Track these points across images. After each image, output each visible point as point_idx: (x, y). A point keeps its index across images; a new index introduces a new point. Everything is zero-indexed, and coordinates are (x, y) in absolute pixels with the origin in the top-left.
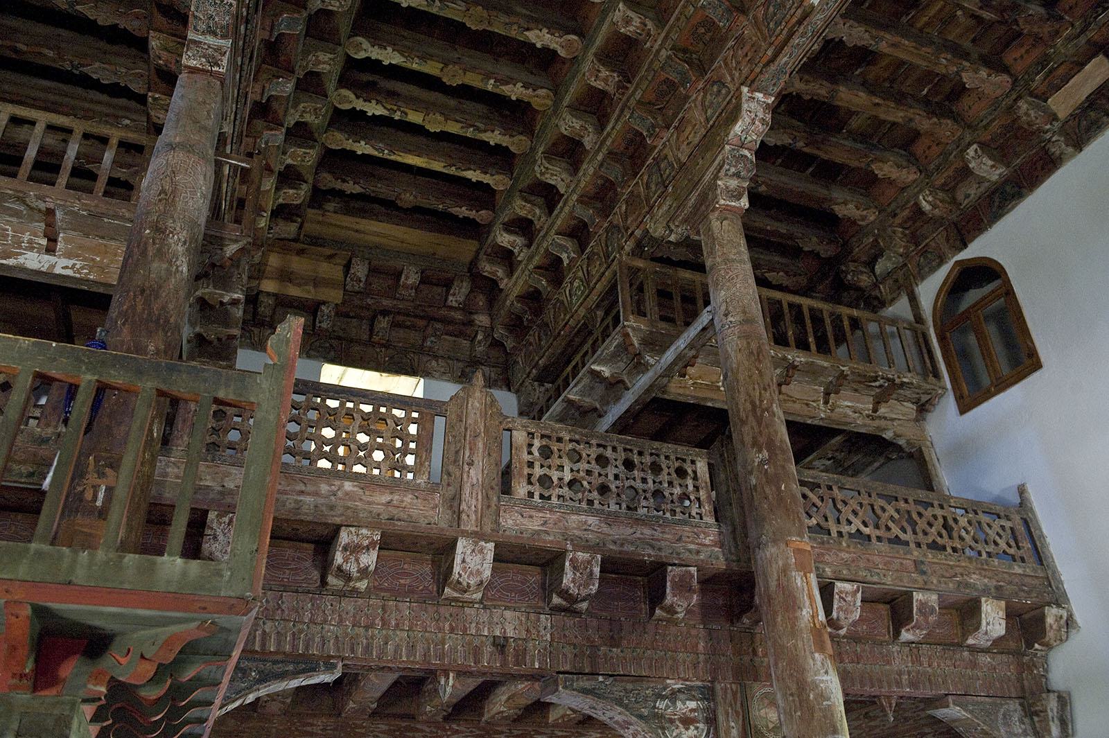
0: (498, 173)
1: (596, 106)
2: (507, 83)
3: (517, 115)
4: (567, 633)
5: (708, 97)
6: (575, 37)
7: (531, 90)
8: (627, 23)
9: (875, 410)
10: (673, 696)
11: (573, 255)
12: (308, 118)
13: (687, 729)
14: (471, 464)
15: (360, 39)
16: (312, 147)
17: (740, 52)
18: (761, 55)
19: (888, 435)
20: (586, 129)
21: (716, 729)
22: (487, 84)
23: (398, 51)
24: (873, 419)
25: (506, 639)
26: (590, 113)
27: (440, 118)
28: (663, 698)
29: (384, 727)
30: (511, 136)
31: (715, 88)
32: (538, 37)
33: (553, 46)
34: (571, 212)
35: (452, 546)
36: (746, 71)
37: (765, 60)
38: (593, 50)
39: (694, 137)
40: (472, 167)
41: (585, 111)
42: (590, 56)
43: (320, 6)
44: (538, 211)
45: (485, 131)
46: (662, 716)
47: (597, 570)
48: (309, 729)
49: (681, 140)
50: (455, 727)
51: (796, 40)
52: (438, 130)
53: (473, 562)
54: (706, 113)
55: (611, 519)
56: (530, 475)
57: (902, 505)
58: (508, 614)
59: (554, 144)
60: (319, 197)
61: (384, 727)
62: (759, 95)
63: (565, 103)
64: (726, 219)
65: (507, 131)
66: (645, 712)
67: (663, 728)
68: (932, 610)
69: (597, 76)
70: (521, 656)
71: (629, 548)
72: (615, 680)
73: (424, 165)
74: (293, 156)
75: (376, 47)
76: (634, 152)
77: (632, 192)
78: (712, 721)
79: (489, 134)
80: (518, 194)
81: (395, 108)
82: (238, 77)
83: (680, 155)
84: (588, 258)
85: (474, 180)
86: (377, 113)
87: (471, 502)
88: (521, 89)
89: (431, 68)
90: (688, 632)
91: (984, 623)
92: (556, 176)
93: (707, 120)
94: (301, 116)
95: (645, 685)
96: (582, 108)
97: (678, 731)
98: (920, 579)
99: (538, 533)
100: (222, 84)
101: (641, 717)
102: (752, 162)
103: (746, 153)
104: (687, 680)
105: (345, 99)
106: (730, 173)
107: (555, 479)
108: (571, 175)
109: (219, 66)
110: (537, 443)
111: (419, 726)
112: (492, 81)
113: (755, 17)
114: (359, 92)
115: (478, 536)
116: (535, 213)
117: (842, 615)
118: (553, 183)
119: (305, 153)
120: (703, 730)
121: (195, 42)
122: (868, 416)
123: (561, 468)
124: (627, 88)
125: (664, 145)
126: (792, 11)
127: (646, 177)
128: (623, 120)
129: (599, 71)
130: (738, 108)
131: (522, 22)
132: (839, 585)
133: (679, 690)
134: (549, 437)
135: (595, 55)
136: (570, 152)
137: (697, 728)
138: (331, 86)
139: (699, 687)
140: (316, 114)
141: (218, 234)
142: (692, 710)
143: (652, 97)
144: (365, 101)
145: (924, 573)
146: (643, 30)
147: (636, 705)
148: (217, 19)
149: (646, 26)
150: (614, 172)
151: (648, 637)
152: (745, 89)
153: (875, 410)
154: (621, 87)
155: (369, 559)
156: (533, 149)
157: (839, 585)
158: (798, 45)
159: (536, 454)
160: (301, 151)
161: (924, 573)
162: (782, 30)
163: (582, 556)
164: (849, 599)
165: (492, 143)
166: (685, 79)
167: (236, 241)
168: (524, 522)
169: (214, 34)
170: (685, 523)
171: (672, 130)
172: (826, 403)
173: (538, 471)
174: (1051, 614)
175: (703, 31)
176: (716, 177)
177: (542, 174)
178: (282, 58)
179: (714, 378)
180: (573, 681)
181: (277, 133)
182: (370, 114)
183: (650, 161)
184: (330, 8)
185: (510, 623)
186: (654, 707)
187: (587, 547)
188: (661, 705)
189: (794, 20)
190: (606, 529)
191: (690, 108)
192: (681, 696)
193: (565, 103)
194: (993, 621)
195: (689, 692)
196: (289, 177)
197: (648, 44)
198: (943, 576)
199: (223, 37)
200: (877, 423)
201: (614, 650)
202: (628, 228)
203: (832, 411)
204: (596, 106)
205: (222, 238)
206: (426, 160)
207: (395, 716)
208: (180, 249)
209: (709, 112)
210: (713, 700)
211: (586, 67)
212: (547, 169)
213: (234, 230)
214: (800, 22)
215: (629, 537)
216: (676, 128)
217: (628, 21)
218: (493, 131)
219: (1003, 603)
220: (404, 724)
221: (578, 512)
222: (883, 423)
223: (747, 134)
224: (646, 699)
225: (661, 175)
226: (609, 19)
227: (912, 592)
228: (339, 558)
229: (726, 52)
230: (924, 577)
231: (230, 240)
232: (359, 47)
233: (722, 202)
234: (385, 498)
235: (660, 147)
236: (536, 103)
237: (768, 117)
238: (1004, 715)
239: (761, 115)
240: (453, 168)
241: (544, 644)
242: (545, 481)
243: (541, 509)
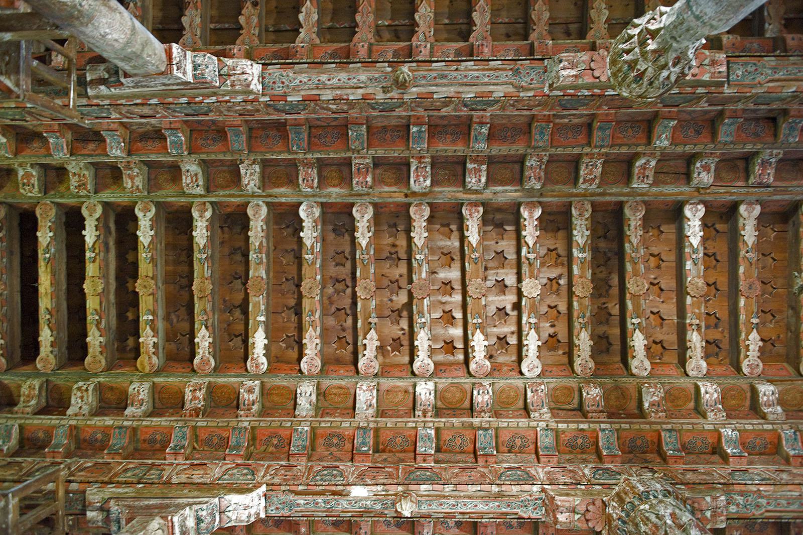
0: (55, 356)
1: (167, 402)
2: (153, 329)
3: (125, 347)
5: (235, 471)
6: (213, 365)
7: (154, 350)
8: (249, 391)
11: (5, 448)
12: (74, 181)
15: (153, 210)
16: (40, 192)
17: (283, 472)
18: (296, 483)
20: (141, 405)
22: (147, 315)
23: (152, 239)
26: (154, 402)
27: (100, 289)
30: (101, 353)
31: (245, 471)
32: (204, 336)
33: (201, 351)
34: (54, 427)
36: (277, 480)
37: (294, 488)
38: (212, 380)
39: (199, 478)
40: (55, 333)
41: (154, 399)
42: (207, 380)
43: (183, 170)
44: (33, 402)
45: (99, 329)
49: (186, 472)
51: (320, 499)
52: (86, 291)
54: (222, 476)
59: (112, 389)
63: (156, 380)
64: (163, 531)
65: (104, 347)
69: (195, 390)
73: (42, 290)
74: (28, 175)
75: (150, 223)
76: (149, 447)
77: (109, 464)
79: (97, 333)
80: (44, 379)
81: (97, 251)
82: (139, 101)
83: (174, 477)
84: (10, 463)
86: (87, 239)
88: (152, 343)
89: (145, 268)
92: (81, 401)
93: (219, 479)
94: (75, 174)
96: (156, 396)
100: (162, 73)
102: (213, 528)
105: (92, 212)
106: (200, 513)
108: (89, 412)
109: (177, 70)
112: (151, 317)
113: (311, 467)
114: (102, 220)
116: (29, 401)
118: (73, 401)
119: (33, 185)
121: (185, 56)
124: (198, 416)
125: (172, 464)
126: (338, 483)
127: (131, 466)
128: (174, 424)
129: (200, 390)
130: (250, 490)
131: (210, 321)
135: (210, 383)
136: (113, 402)
138: (107, 196)
140: (79, 186)
141: (21, 70)
143: (203, 436)
144: (96, 226)
146: (248, 405)
148: (207, 70)
149: (253, 405)
150: (118, 441)
152: (264, 488)
154: (197, 412)
156: (96, 375)
158: (317, 504)
160: (35, 181)
162: (322, 485)
165: (88, 339)
166: (237, 447)
167: (17, 85)
169: (195, 68)
171: (188, 462)
175: (275, 443)
176: (190, 505)
177: (79, 389)
178: (139, 144)
181: (66, 151)
182: (84, 233)
183: (150, 462)
184: (184, 177)
189: (334, 488)
191: (216, 464)
193: (156, 380)
197: (242, 413)
199: (194, 76)
202: (73, 476)
204: (167, 402)
206: (49, 291)
209: (226, 477)
211: (195, 380)
212: (87, 390)
213: (26, 83)
214: (334, 493)
216: (192, 465)
217: (250, 391)
218: (101, 336)
223: (235, 509)
225: (145, 474)
226: (242, 379)
229: (276, 464)
231: (18, 80)
232: (146, 210)
233: (175, 519)
235: (167, 462)
236: (143, 360)
237: (253, 519)
239: (253, 511)
240: (48, 317)
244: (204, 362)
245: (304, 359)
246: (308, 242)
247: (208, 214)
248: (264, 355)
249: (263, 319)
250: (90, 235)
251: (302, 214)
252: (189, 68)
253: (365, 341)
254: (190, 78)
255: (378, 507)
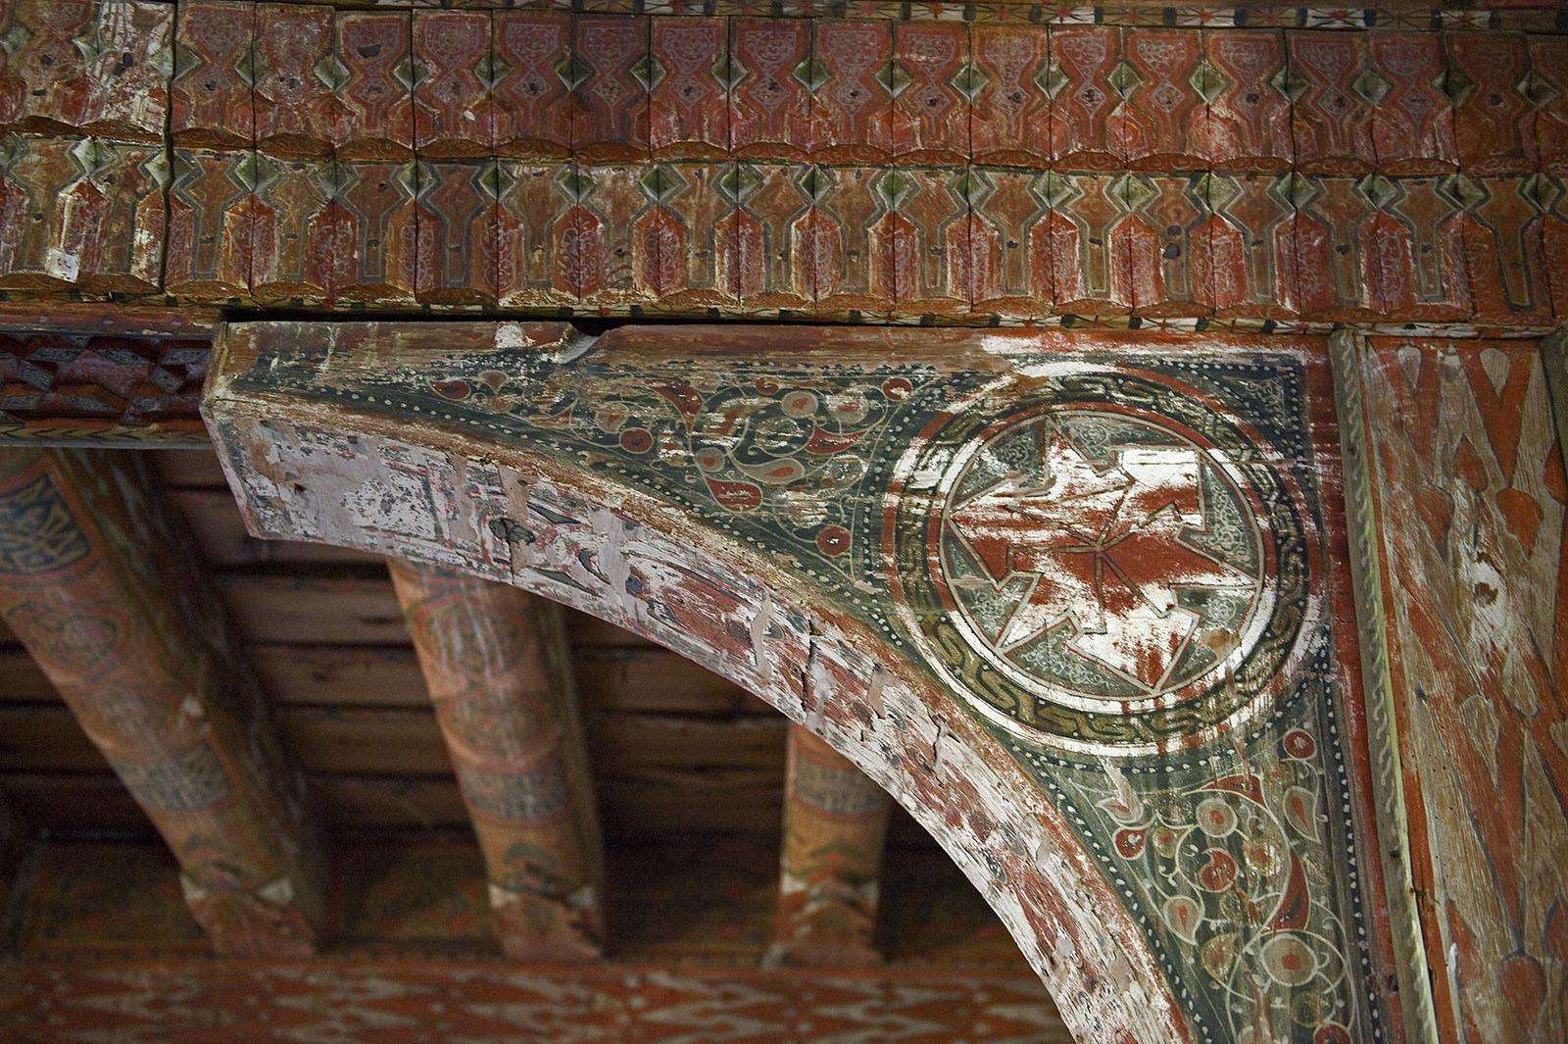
4: (267, 87)
10: (1027, 424)
13: (1118, 604)
21: (1346, 606)
28: (945, 432)
29: (383, 988)
46: (934, 529)
48: (102, 1003)
50: (661, 979)
61: (383, 988)
66: (809, 509)
67: (935, 600)
72: (620, 345)
78: (1309, 554)
90: (1121, 52)
95: (820, 363)
97: (1046, 615)
101: (771, 536)
104: (1133, 332)
111: (520, 980)
120: (1242, 611)
133: (1073, 392)
137: (1197, 599)
139: (1218, 373)
142: (1154, 501)
147: (748, 474)
151: (830, 100)
180: (315, 351)
186: (881, 482)
188: (928, 471)
192: (1087, 422)
195: (1149, 406)
201: (605, 174)
207: (429, 947)
210: (1329, 439)
220: (461, 975)
224: (819, 440)
241: (119, 156)
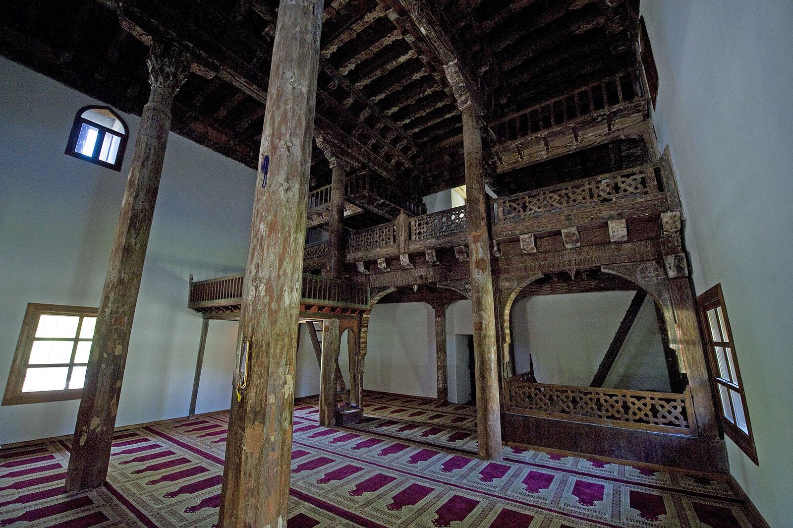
6: (424, 68)
9: (610, 129)
14: (401, 235)
19: (623, 137)
24: (609, 135)
25: (422, 276)
35: (398, 258)
47: (434, 254)
53: (405, 260)
55: (438, 238)
56: (416, 233)
57: (564, 192)
58: (422, 269)
60: (422, 147)
62: (451, 63)
68: (574, 234)
70: (427, 279)
71: (443, 245)
79: (438, 105)
85: (450, 117)
87: (402, 245)
91: (611, 232)
98: (567, 223)
99: (418, 248)
103: (462, 84)
107: (422, 232)
110: (417, 223)
115: (404, 253)
117: (525, 247)
122: (605, 135)
123: (423, 228)
132: (522, 237)
134: (420, 220)
145: (570, 219)
153: (610, 129)
155: (384, 265)
157: (522, 237)
159: (417, 226)
161: (570, 219)
163: (429, 251)
164: (528, 240)
165: (441, 106)
168: (414, 247)
170: (461, 232)
172: (577, 140)
173: (418, 231)
174: (666, 217)
179: (516, 158)
185: (422, 271)
187: (432, 249)
190: (437, 241)
194: (618, 230)
196: (405, 150)
198: (582, 218)
200: (612, 135)
203: (580, 143)
205: (364, 195)
208: (335, 213)
214: (430, 41)
215: (442, 242)
219: (624, 221)
221: (429, 239)
222: (616, 134)
227: (560, 230)
228: (379, 266)
230: (570, 222)
234: (385, 250)
238: (642, 269)
242: (420, 233)
243: (419, 241)
244: (425, 71)
245: (398, 38)
246: (354, 65)
247: (374, 98)
248: (408, 54)
249: (394, 63)
250: (408, 121)
251: (347, 73)
252: (332, 159)
253: (372, 20)
254: (334, 158)
255: (424, 20)
